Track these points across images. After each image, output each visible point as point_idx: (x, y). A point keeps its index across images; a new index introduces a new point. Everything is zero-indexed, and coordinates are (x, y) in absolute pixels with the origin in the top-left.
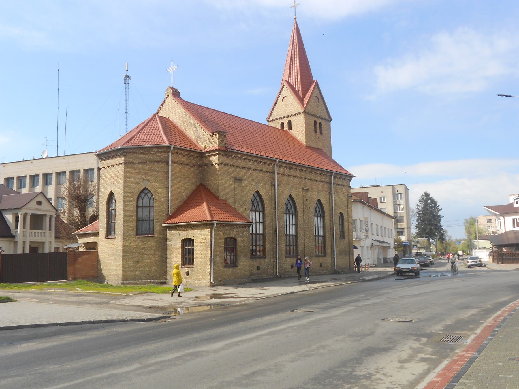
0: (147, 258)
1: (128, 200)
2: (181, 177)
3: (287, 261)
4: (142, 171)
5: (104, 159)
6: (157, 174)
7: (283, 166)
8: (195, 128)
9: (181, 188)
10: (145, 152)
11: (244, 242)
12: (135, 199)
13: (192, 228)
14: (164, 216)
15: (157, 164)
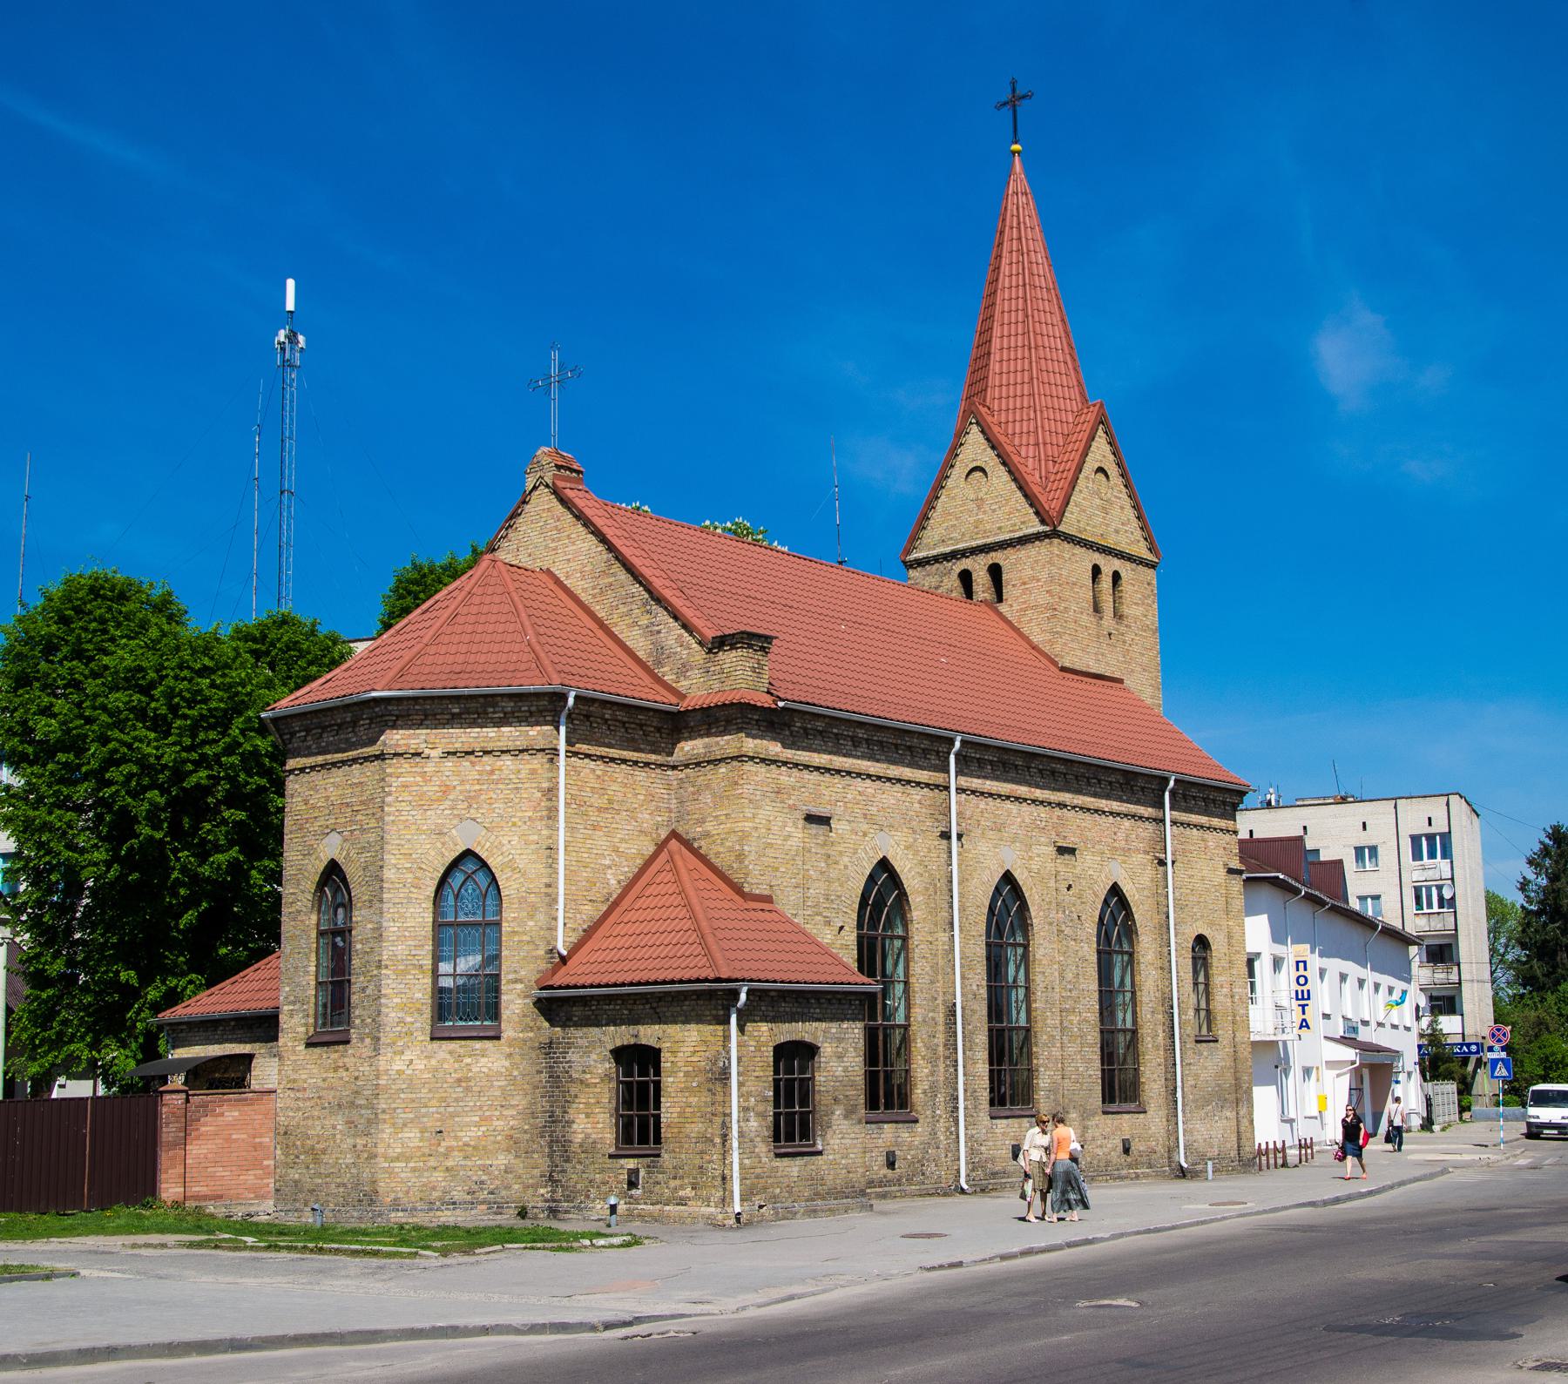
0: (477, 1119)
1: (402, 895)
2: (600, 810)
3: (997, 1131)
4: (455, 787)
5: (303, 734)
6: (512, 796)
7: (978, 759)
8: (648, 616)
9: (599, 852)
10: (469, 713)
11: (845, 1059)
12: (428, 893)
13: (655, 1005)
14: (536, 958)
15: (511, 758)
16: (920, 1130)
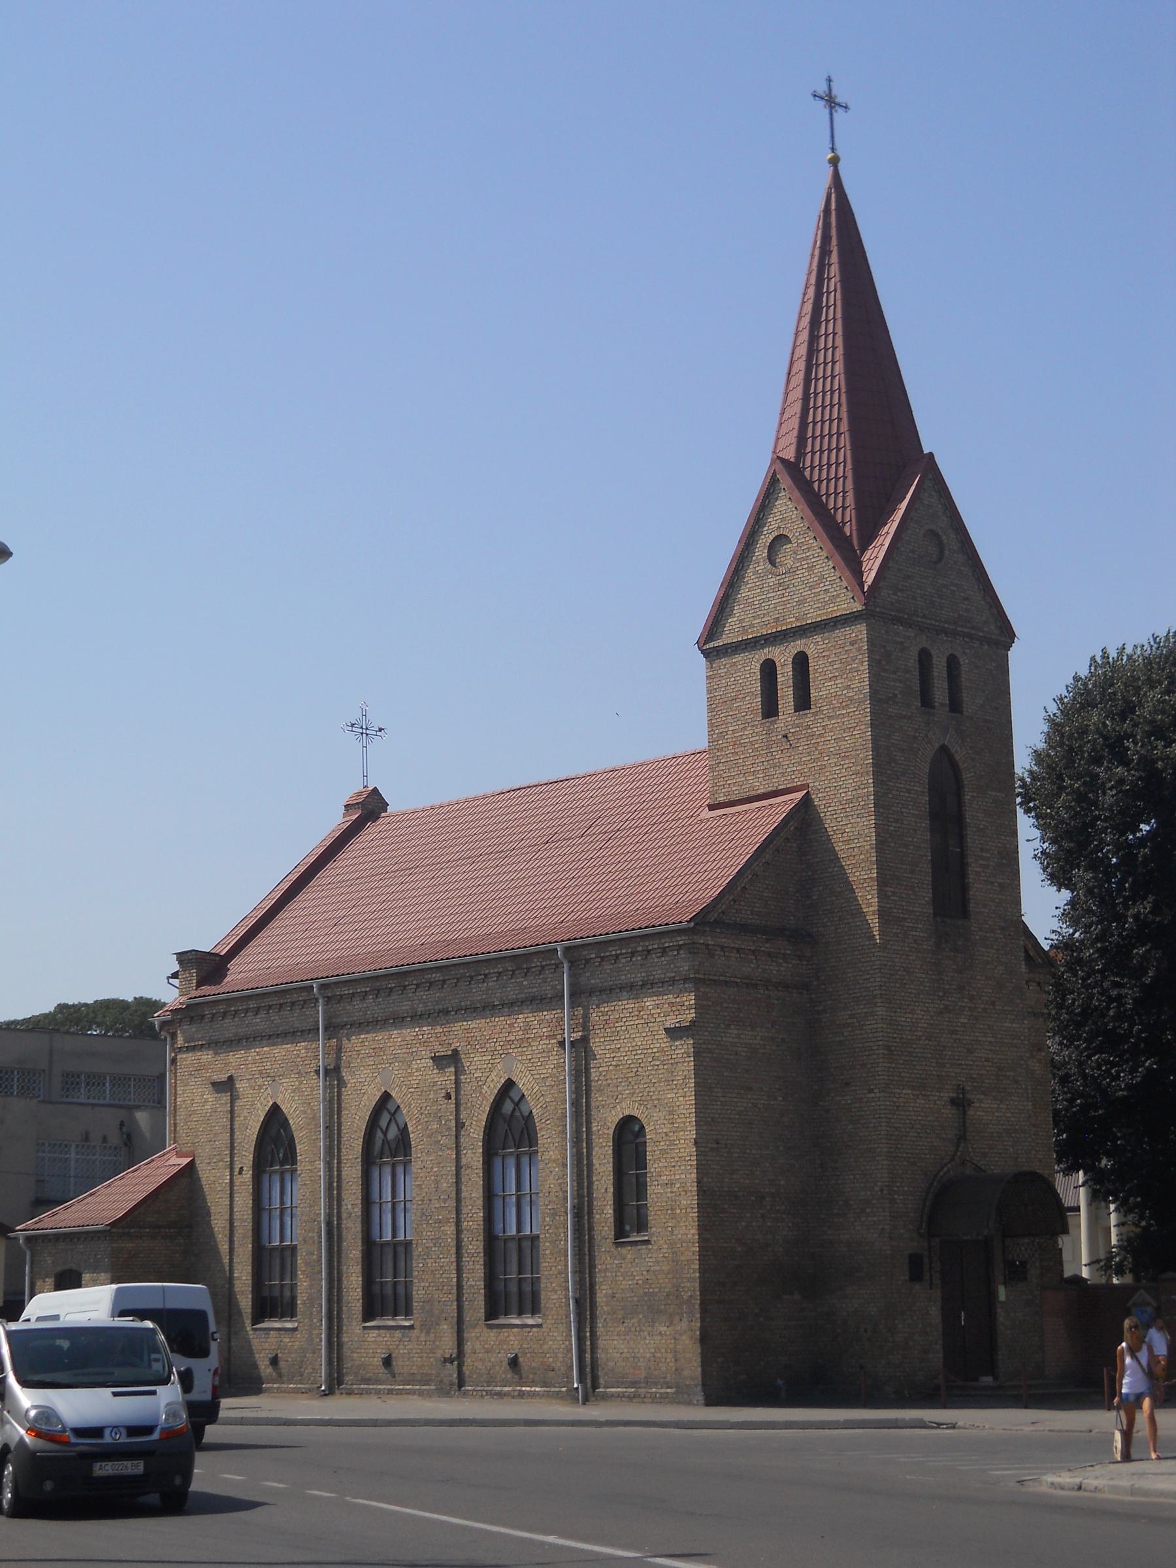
16: (298, 1336)
